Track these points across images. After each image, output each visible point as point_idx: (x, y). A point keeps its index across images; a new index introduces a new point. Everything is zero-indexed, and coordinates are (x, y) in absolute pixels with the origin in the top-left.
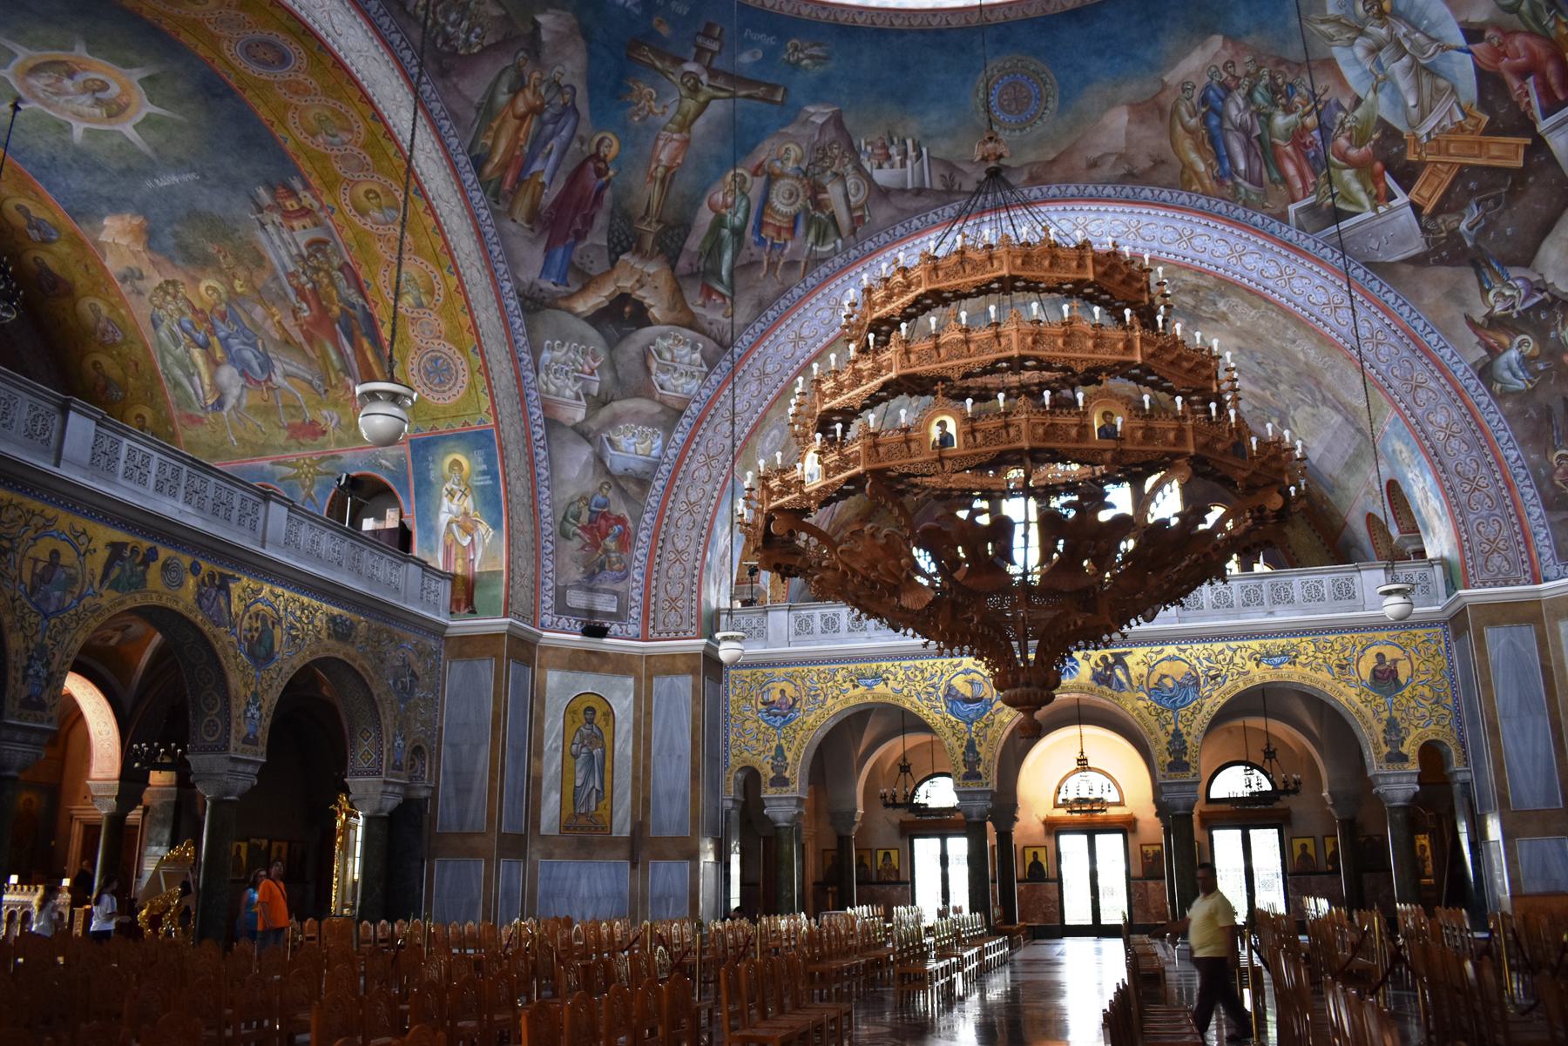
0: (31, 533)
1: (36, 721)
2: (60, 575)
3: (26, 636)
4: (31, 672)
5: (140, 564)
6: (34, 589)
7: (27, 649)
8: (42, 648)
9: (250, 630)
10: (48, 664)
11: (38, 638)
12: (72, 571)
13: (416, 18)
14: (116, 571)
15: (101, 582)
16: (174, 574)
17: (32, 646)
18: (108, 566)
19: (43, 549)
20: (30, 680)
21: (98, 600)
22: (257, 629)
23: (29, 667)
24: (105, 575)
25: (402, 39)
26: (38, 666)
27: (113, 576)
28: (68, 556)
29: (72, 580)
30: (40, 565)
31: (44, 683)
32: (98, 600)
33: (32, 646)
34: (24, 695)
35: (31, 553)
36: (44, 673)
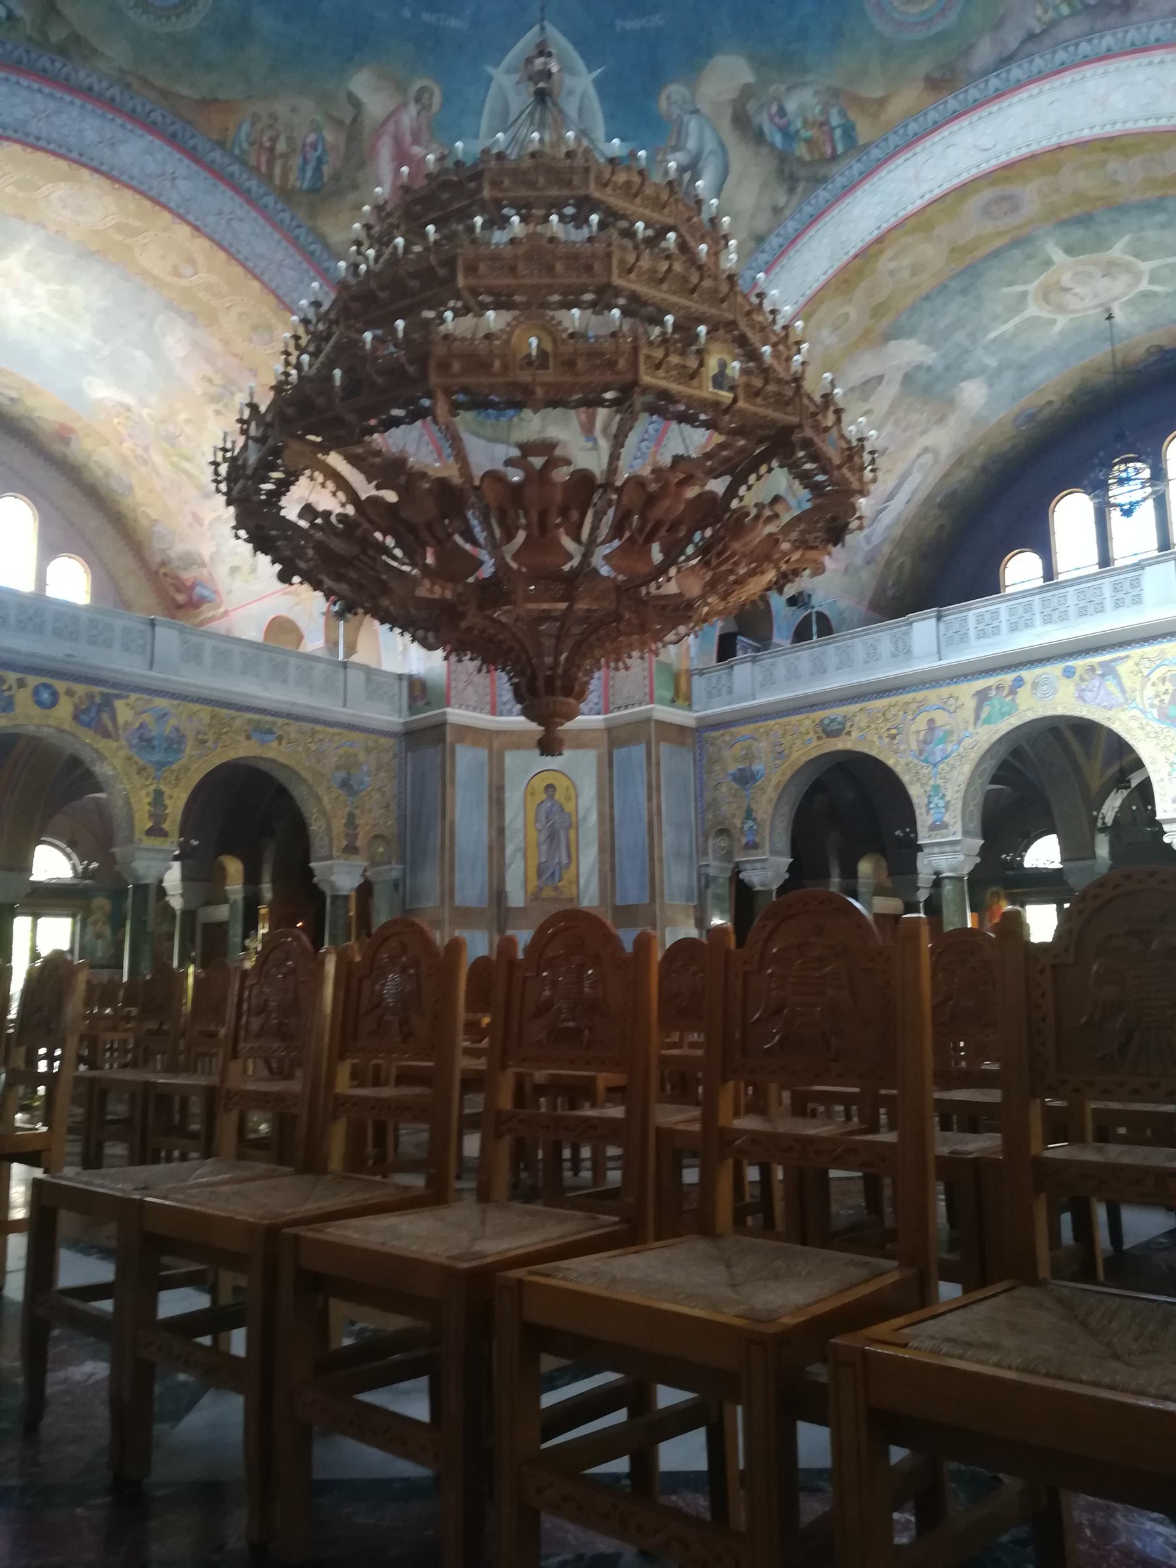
0: (910, 717)
1: (943, 837)
2: (939, 734)
3: (922, 784)
4: (932, 806)
5: (1007, 695)
6: (921, 752)
7: (925, 791)
8: (937, 788)
9: (1157, 696)
10: (944, 796)
11: (932, 782)
12: (947, 727)
13: (1053, 24)
14: (986, 710)
15: (975, 724)
16: (1045, 688)
17: (928, 788)
18: (978, 710)
19: (921, 724)
20: (932, 812)
21: (976, 738)
22: (1166, 692)
23: (930, 803)
24: (977, 717)
25: (1066, 48)
26: (936, 800)
27: (983, 716)
28: (940, 717)
29: (950, 733)
30: (922, 734)
31: (943, 810)
32: (976, 738)
33: (928, 788)
34: (930, 822)
35: (913, 728)
36: (942, 803)
